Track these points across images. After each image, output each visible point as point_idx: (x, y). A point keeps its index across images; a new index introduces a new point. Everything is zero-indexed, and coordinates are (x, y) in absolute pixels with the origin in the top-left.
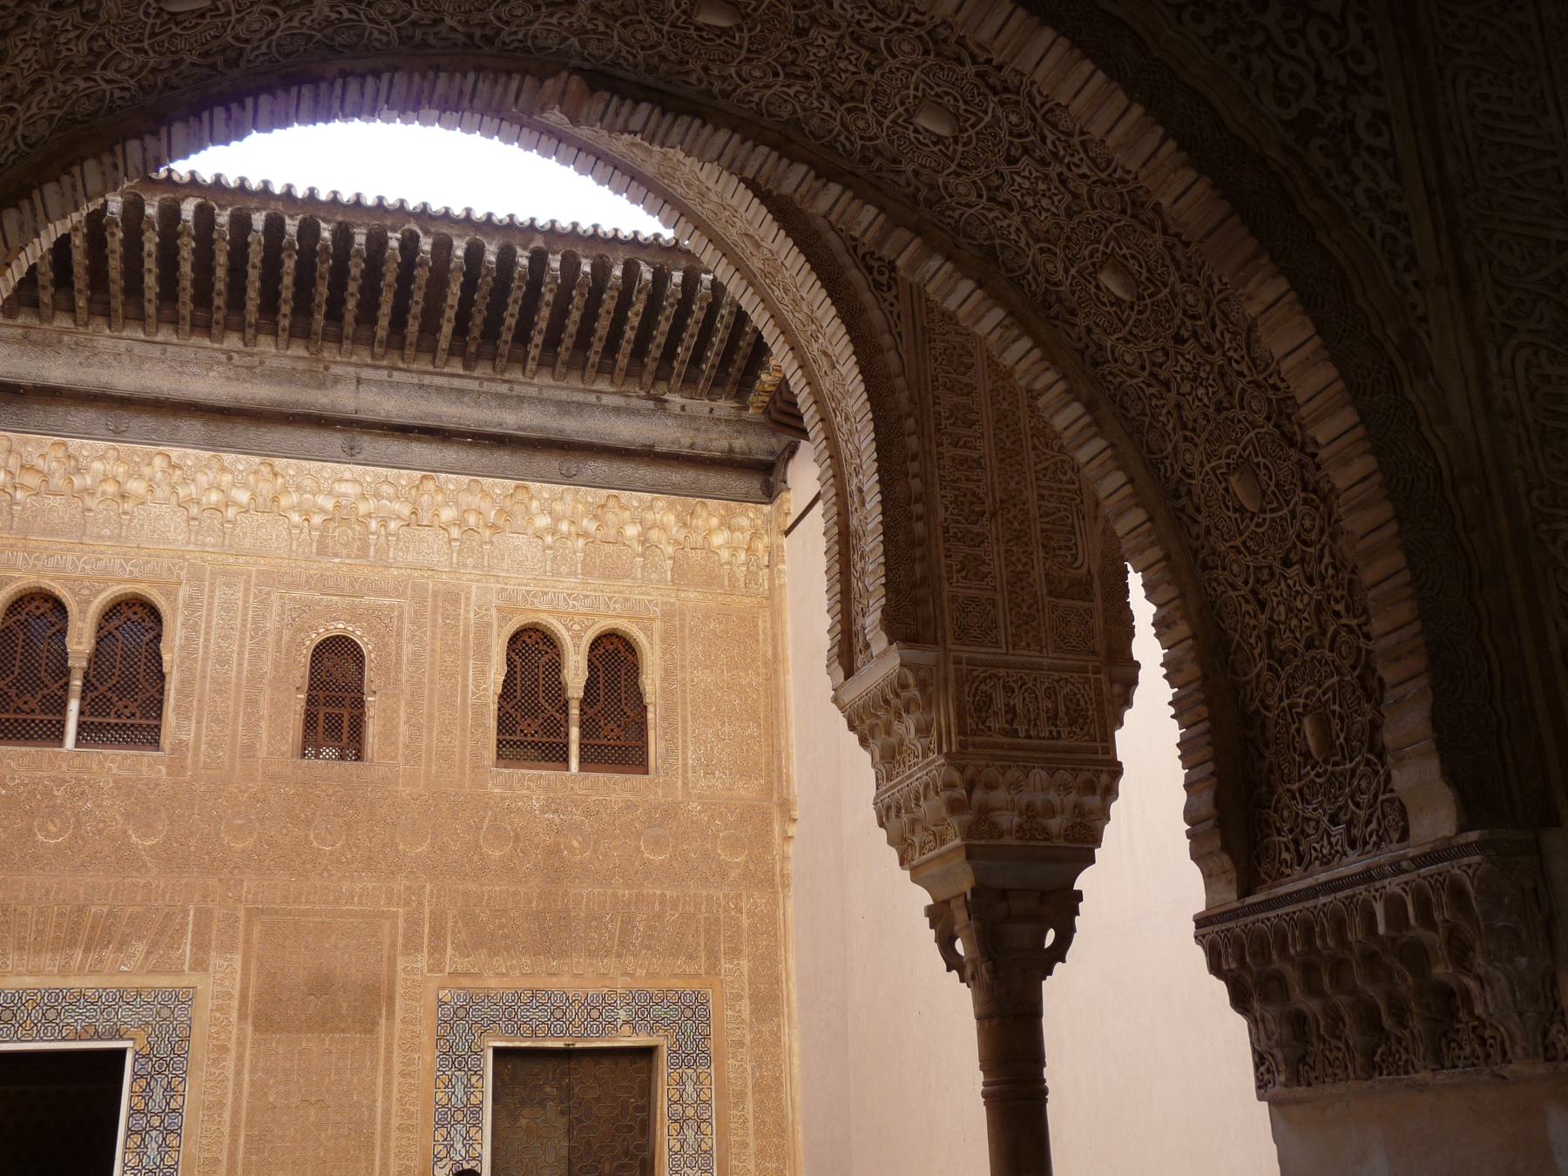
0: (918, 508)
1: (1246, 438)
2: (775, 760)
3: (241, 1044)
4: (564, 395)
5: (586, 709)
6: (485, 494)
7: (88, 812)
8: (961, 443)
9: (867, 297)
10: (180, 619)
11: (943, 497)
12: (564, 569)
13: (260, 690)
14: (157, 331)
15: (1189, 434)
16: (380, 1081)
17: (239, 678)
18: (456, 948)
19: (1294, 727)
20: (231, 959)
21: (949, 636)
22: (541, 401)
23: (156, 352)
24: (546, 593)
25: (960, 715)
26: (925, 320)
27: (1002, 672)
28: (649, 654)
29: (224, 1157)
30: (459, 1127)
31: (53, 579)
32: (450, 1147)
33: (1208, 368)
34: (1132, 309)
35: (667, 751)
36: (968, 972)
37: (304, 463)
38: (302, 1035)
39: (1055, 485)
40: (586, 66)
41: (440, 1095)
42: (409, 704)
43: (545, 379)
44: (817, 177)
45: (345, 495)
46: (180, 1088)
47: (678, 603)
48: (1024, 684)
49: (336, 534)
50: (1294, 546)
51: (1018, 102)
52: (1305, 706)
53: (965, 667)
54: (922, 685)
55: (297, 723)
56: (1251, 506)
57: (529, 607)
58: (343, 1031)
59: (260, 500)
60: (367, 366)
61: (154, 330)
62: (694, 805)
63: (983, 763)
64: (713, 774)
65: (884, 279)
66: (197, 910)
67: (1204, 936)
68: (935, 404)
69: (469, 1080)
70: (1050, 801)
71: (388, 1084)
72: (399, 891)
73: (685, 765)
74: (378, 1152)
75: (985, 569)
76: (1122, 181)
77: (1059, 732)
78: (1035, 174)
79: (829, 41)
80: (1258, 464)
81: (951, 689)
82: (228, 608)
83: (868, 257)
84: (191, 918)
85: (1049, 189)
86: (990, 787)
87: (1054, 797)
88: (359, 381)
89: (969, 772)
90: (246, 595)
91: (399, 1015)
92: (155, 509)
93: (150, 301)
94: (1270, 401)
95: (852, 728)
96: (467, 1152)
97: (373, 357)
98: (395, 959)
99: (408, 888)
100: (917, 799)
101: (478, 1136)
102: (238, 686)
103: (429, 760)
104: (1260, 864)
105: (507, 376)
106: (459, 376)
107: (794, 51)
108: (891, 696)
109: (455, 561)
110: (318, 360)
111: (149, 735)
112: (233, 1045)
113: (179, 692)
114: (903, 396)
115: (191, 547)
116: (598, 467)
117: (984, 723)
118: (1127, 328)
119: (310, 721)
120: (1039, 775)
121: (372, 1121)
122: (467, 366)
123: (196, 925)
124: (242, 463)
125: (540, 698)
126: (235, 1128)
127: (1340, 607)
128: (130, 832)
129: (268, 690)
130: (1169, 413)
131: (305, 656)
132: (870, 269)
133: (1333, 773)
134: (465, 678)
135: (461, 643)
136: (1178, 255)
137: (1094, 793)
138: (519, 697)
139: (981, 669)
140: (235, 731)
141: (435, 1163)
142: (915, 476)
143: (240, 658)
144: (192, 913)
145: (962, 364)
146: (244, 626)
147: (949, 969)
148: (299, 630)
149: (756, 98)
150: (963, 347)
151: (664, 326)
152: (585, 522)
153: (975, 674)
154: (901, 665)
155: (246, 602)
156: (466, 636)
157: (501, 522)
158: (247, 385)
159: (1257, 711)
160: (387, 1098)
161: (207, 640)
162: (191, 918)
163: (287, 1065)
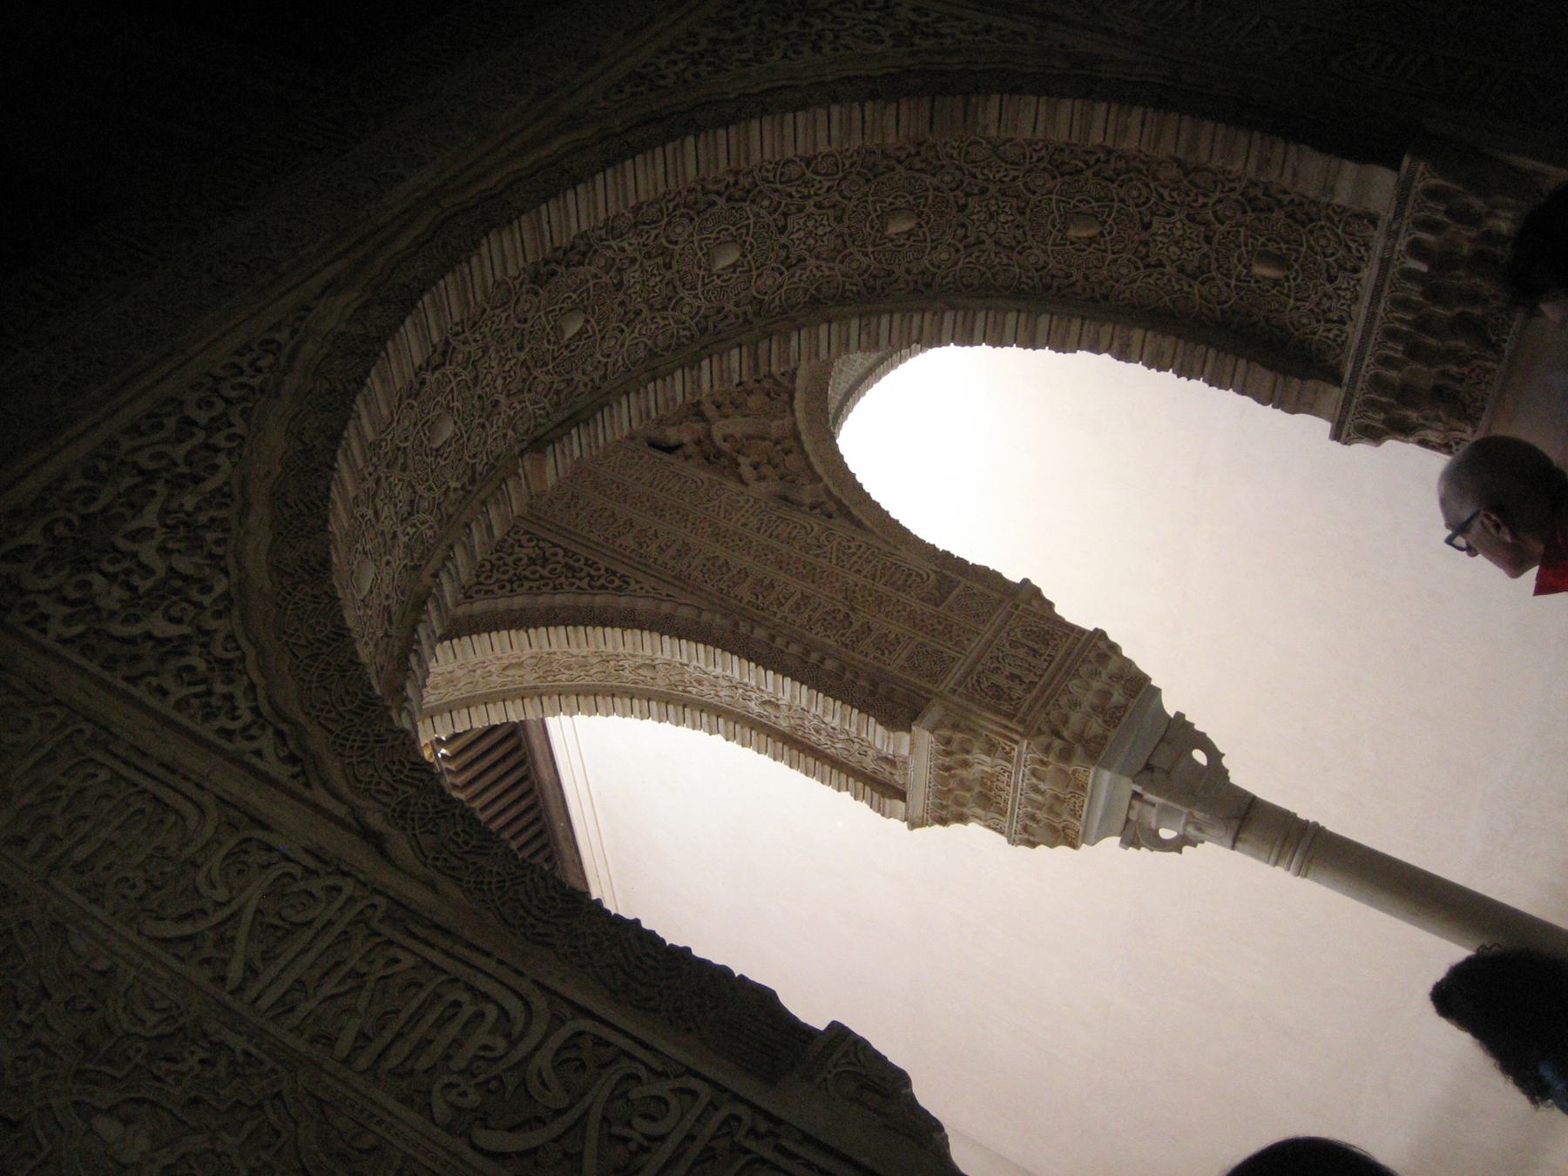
0: (814, 657)
1: (1053, 204)
8: (783, 600)
9: (624, 602)
11: (817, 634)
15: (1019, 248)
19: (1253, 284)
21: (929, 686)
25: (998, 712)
26: (669, 572)
27: (979, 667)
33: (993, 202)
34: (921, 227)
36: (1191, 831)
39: (855, 558)
40: (525, 444)
44: (692, 368)
48: (997, 658)
50: (1140, 213)
51: (760, 192)
52: (1245, 266)
53: (961, 689)
54: (956, 727)
56: (1093, 232)
63: (1044, 716)
65: (617, 583)
67: (1349, 435)
68: (740, 601)
70: (1099, 691)
75: (892, 636)
76: (852, 165)
77: (1048, 656)
78: (801, 222)
79: (636, 275)
80: (1075, 206)
81: (975, 708)
83: (592, 583)
85: (816, 221)
86: (1065, 721)
87: (1097, 685)
89: (1045, 728)
94: (1044, 169)
95: (943, 821)
100: (1036, 790)
104: (1326, 361)
107: (622, 304)
108: (947, 761)
114: (718, 620)
117: (1013, 700)
118: (929, 240)
120: (1074, 684)
127: (1201, 200)
130: (996, 254)
132: (603, 587)
133: (1302, 265)
136: (919, 166)
137: (1110, 658)
139: (969, 679)
142: (787, 646)
145: (720, 568)
147: (1180, 852)
149: (620, 362)
150: (708, 560)
153: (970, 686)
154: (932, 732)
159: (1223, 311)
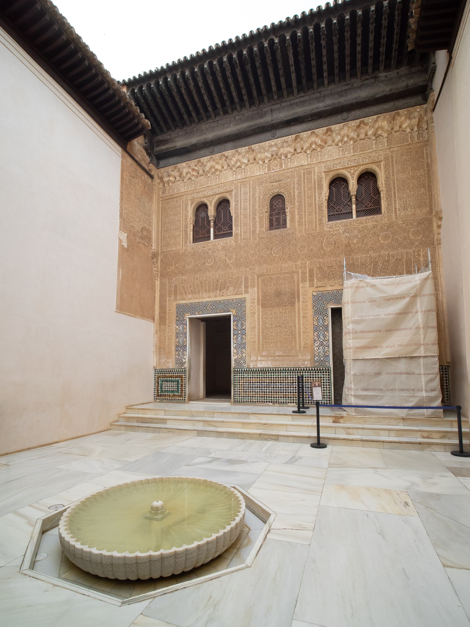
2: (433, 200)
3: (259, 312)
4: (339, 89)
5: (358, 199)
6: (317, 136)
7: (217, 256)
10: (233, 200)
12: (346, 153)
13: (256, 215)
14: (215, 118)
16: (297, 320)
17: (250, 213)
18: (317, 279)
20: (254, 289)
22: (332, 94)
23: (216, 124)
24: (340, 163)
28: (380, 174)
29: (257, 340)
30: (321, 331)
31: (204, 197)
32: (319, 337)
35: (388, 205)
37: (261, 144)
38: (274, 308)
41: (315, 323)
42: (298, 209)
43: (333, 86)
45: (274, 151)
46: (245, 324)
47: (390, 153)
49: (273, 164)
55: (267, 222)
57: (335, 169)
58: (285, 306)
59: (251, 160)
60: (274, 105)
61: (214, 118)
62: (400, 222)
64: (407, 209)
66: (245, 277)
69: (324, 318)
71: (299, 320)
72: (299, 265)
73: (396, 209)
74: (297, 339)
82: (245, 193)
84: (243, 280)
88: (272, 111)
90: (250, 189)
91: (301, 301)
92: (225, 172)
93: (209, 106)
96: (324, 339)
97: (275, 101)
98: (299, 285)
99: (301, 264)
101: (327, 334)
102: (250, 215)
103: (305, 224)
105: (319, 90)
106: (303, 96)
109: (309, 160)
110: (259, 109)
111: (230, 234)
112: (256, 312)
113: (235, 220)
115: (234, 179)
116: (357, 113)
119: (271, 221)
121: (295, 330)
122: (304, 92)
123: (245, 281)
124: (243, 150)
125: (342, 200)
126: (259, 333)
128: (227, 259)
129: (258, 214)
131: (267, 203)
134: (315, 197)
135: (313, 186)
138: (335, 201)
140: (250, 228)
141: (315, 342)
143: (250, 207)
144: (243, 278)
146: (250, 197)
148: (264, 195)
151: (371, 37)
152: (352, 134)
155: (250, 191)
156: (315, 183)
157: (323, 144)
158: (241, 125)
160: (299, 324)
161: (241, 204)
162: (243, 280)
163: (271, 316)
